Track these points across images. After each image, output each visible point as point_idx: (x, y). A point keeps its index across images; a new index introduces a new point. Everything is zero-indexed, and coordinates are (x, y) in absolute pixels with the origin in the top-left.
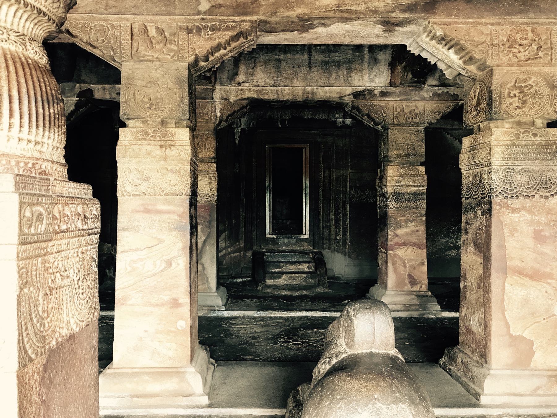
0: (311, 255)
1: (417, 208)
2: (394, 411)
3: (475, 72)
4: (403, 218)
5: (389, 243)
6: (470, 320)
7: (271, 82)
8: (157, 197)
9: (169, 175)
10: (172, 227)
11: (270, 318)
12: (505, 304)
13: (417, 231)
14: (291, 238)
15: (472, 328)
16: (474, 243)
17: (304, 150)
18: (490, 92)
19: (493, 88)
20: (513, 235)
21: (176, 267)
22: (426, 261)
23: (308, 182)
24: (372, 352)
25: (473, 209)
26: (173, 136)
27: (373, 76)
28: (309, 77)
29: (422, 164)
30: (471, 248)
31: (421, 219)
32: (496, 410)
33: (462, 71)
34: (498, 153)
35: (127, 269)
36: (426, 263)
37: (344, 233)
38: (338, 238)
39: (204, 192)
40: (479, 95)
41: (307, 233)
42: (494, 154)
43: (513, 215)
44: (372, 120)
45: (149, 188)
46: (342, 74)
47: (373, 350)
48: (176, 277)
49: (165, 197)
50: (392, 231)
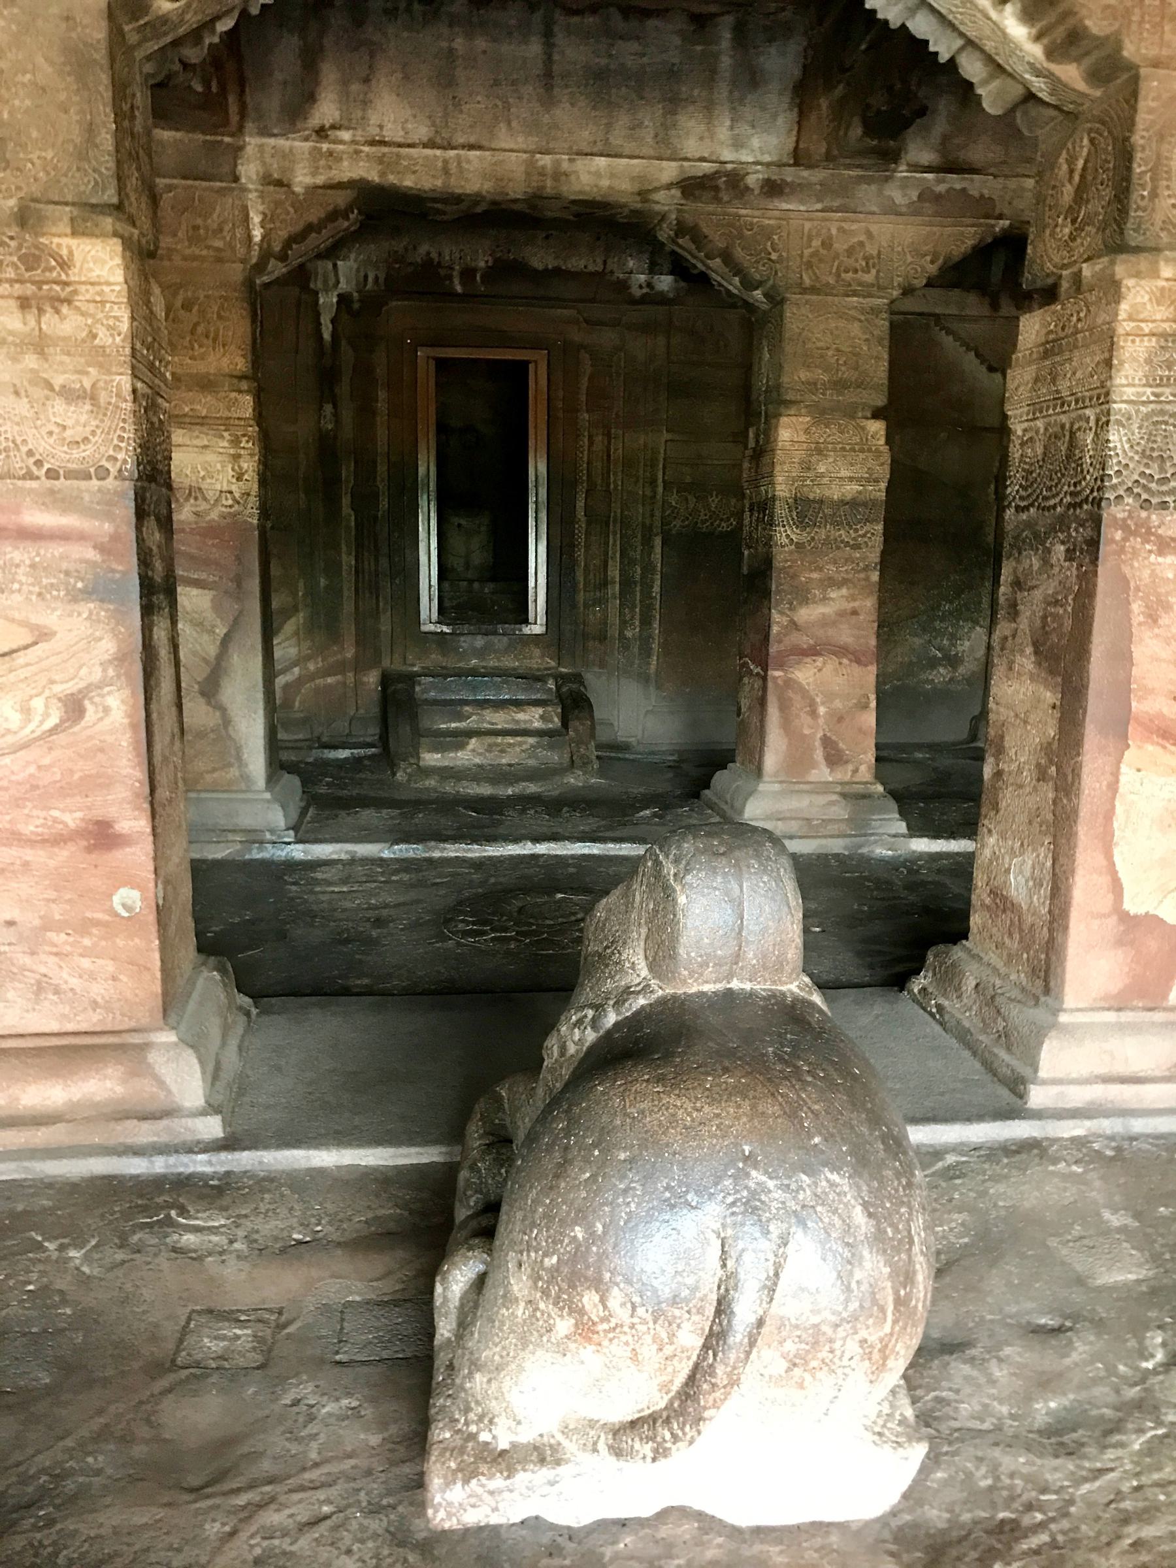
0: (551, 684)
1: (856, 547)
2: (806, 1196)
3: (1081, 86)
4: (815, 575)
5: (773, 649)
6: (1008, 871)
7: (422, 132)
8: (20, 483)
9: (58, 406)
10: (80, 585)
11: (430, 861)
12: (1115, 825)
13: (855, 613)
14: (495, 633)
15: (1013, 893)
16: (1036, 644)
17: (531, 367)
18: (1126, 155)
19: (1137, 139)
20: (1155, 621)
21: (101, 719)
22: (873, 697)
23: (543, 468)
24: (729, 993)
25: (1039, 540)
26: (64, 265)
27: (744, 129)
28: (546, 119)
29: (876, 415)
30: (1026, 661)
31: (867, 579)
32: (1070, 1123)
33: (1039, 85)
34: (1135, 360)
36: (873, 704)
37: (646, 621)
38: (629, 634)
39: (218, 487)
40: (1084, 169)
41: (541, 618)
42: (1122, 363)
43: (1160, 559)
44: (738, 270)
46: (650, 117)
47: (735, 984)
48: (102, 750)
49: (49, 483)
50: (782, 613)
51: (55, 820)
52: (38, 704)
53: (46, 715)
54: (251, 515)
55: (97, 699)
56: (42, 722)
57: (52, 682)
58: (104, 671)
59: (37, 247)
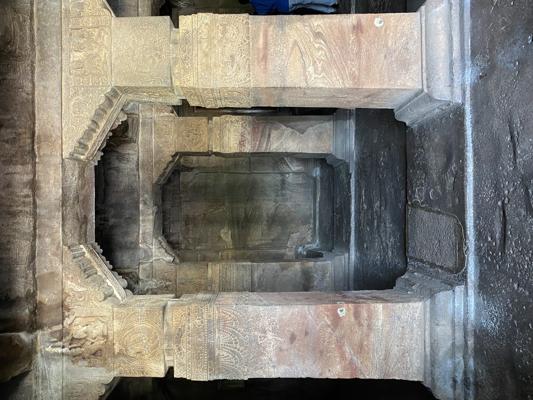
9: (227, 35)
26: (187, 32)
35: (324, 77)
39: (240, 128)
45: (241, 56)
48: (331, 27)
51: (353, 42)
52: (317, 46)
53: (320, 43)
54: (249, 118)
55: (315, 28)
56: (323, 45)
57: (310, 41)
58: (306, 26)
59: (183, 40)
